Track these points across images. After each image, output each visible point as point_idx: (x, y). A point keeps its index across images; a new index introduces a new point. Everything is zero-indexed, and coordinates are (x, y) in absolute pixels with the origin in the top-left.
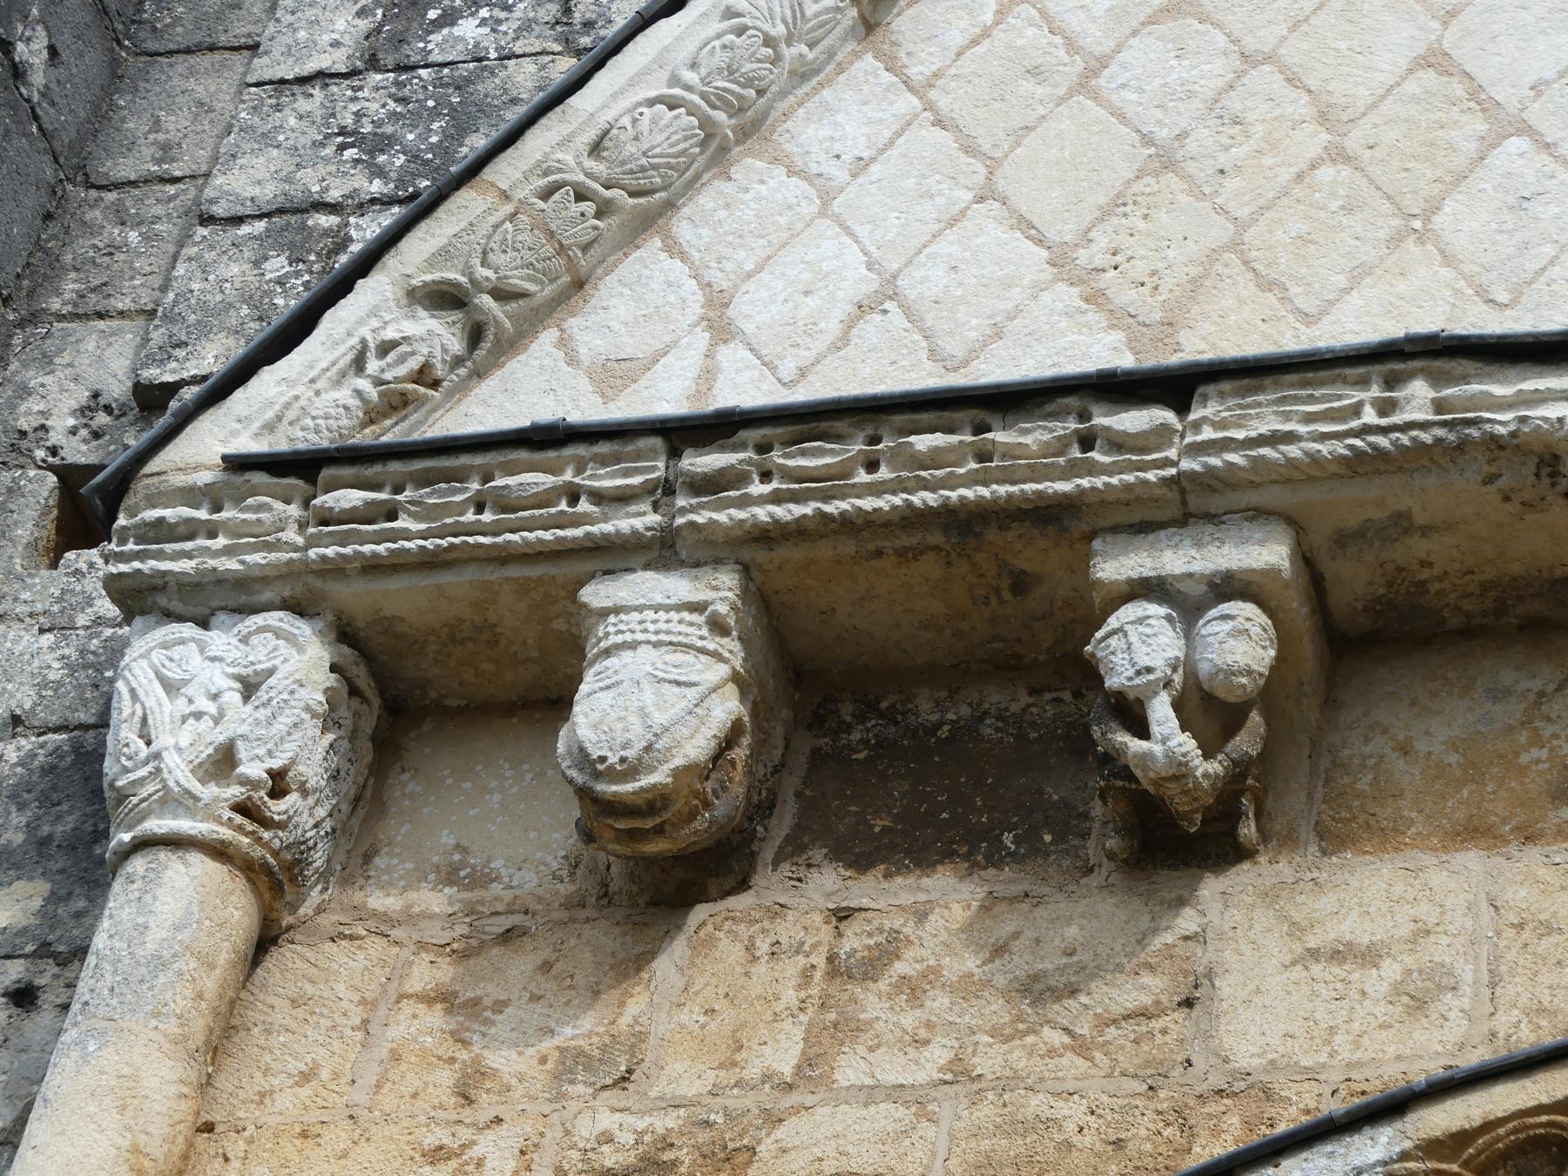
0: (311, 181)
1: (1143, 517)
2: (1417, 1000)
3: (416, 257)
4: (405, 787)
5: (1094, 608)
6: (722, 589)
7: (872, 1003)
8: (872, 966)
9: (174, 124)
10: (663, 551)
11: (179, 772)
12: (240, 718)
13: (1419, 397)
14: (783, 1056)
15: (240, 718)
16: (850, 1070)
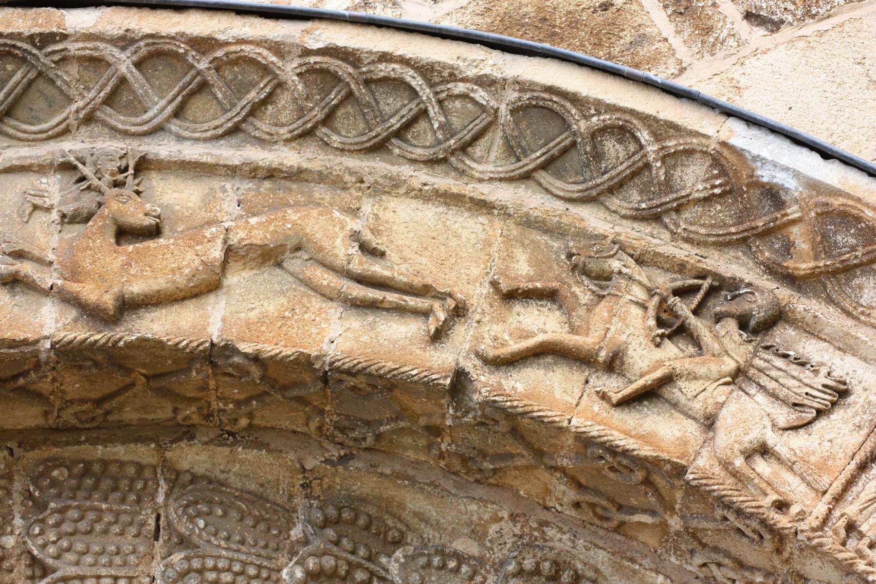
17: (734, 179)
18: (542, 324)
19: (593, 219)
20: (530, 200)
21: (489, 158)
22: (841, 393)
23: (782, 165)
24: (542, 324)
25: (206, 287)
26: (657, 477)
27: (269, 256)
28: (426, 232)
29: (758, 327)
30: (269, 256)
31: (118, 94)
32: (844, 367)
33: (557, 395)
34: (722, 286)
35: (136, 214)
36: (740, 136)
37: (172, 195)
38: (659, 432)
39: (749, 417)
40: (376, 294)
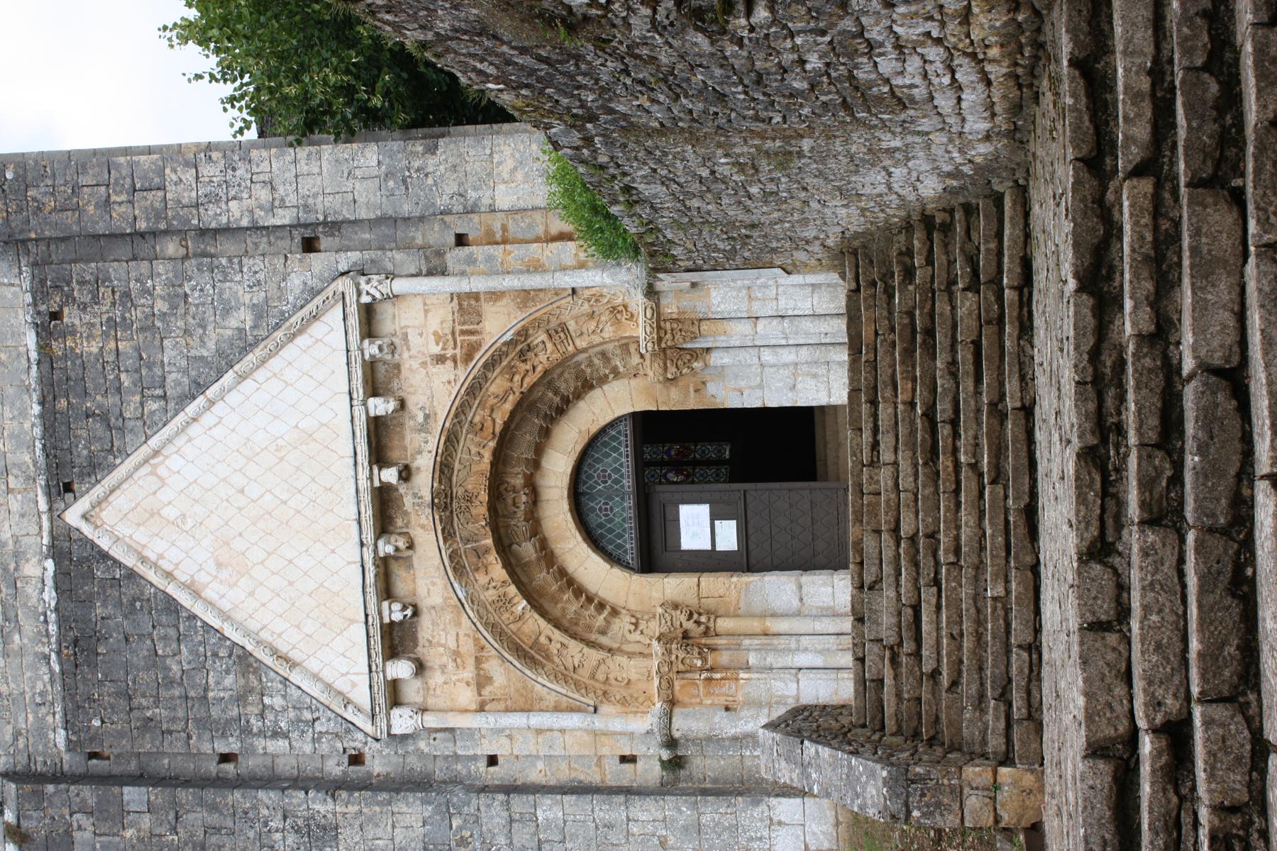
0: (309, 739)
1: (381, 618)
2: (434, 584)
3: (341, 711)
4: (406, 701)
5: (392, 623)
6: (389, 664)
7: (435, 641)
8: (430, 642)
9: (288, 768)
10: (384, 671)
11: (413, 722)
12: (405, 716)
13: (368, 590)
14: (442, 649)
15: (405, 716)
16: (443, 641)
17: (507, 344)
18: (517, 378)
19: (504, 363)
20: (498, 371)
21: (489, 375)
22: (543, 342)
23: (508, 337)
24: (517, 378)
25: (494, 421)
26: (546, 372)
27: (492, 410)
28: (497, 385)
29: (529, 348)
30: (492, 410)
31: (459, 423)
32: (539, 340)
33: (529, 380)
34: (521, 351)
35: (479, 426)
36: (502, 341)
37: (477, 419)
38: (539, 369)
39: (543, 357)
40: (504, 399)
